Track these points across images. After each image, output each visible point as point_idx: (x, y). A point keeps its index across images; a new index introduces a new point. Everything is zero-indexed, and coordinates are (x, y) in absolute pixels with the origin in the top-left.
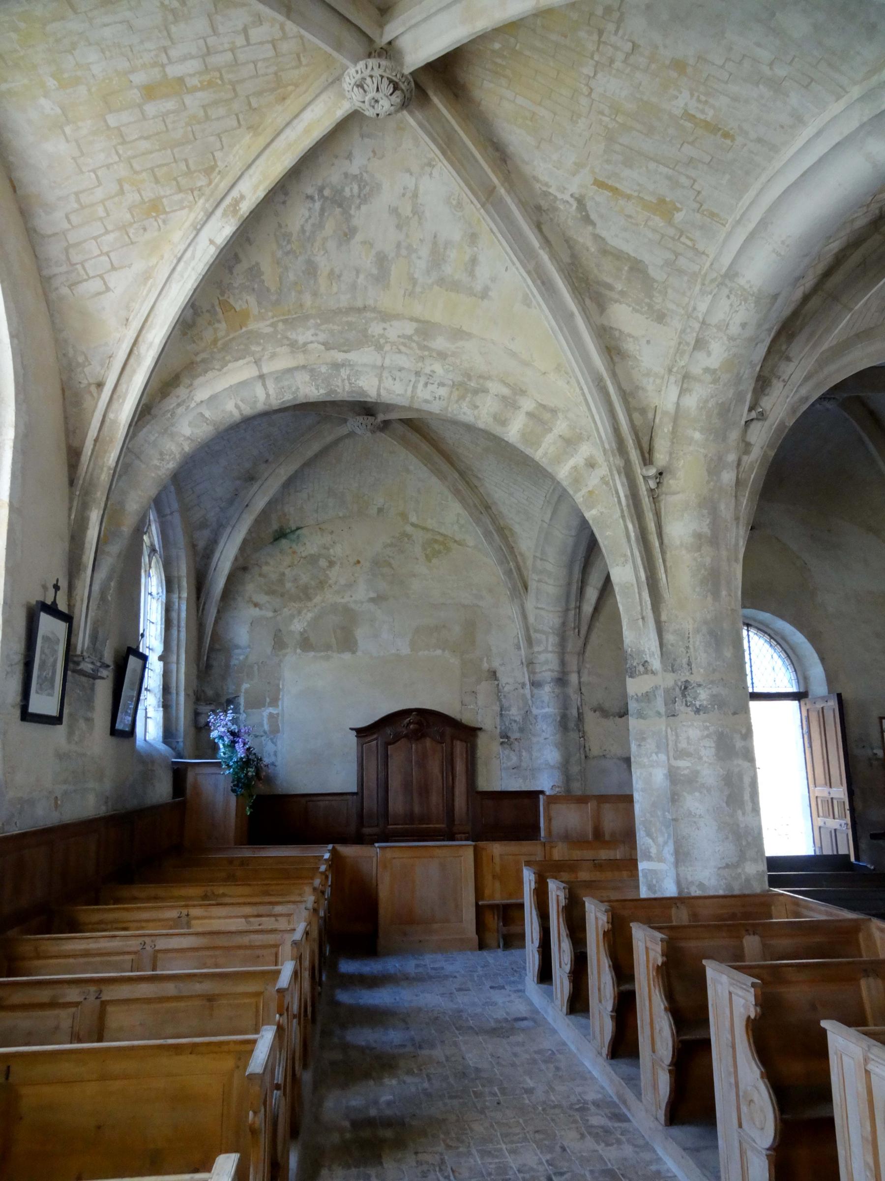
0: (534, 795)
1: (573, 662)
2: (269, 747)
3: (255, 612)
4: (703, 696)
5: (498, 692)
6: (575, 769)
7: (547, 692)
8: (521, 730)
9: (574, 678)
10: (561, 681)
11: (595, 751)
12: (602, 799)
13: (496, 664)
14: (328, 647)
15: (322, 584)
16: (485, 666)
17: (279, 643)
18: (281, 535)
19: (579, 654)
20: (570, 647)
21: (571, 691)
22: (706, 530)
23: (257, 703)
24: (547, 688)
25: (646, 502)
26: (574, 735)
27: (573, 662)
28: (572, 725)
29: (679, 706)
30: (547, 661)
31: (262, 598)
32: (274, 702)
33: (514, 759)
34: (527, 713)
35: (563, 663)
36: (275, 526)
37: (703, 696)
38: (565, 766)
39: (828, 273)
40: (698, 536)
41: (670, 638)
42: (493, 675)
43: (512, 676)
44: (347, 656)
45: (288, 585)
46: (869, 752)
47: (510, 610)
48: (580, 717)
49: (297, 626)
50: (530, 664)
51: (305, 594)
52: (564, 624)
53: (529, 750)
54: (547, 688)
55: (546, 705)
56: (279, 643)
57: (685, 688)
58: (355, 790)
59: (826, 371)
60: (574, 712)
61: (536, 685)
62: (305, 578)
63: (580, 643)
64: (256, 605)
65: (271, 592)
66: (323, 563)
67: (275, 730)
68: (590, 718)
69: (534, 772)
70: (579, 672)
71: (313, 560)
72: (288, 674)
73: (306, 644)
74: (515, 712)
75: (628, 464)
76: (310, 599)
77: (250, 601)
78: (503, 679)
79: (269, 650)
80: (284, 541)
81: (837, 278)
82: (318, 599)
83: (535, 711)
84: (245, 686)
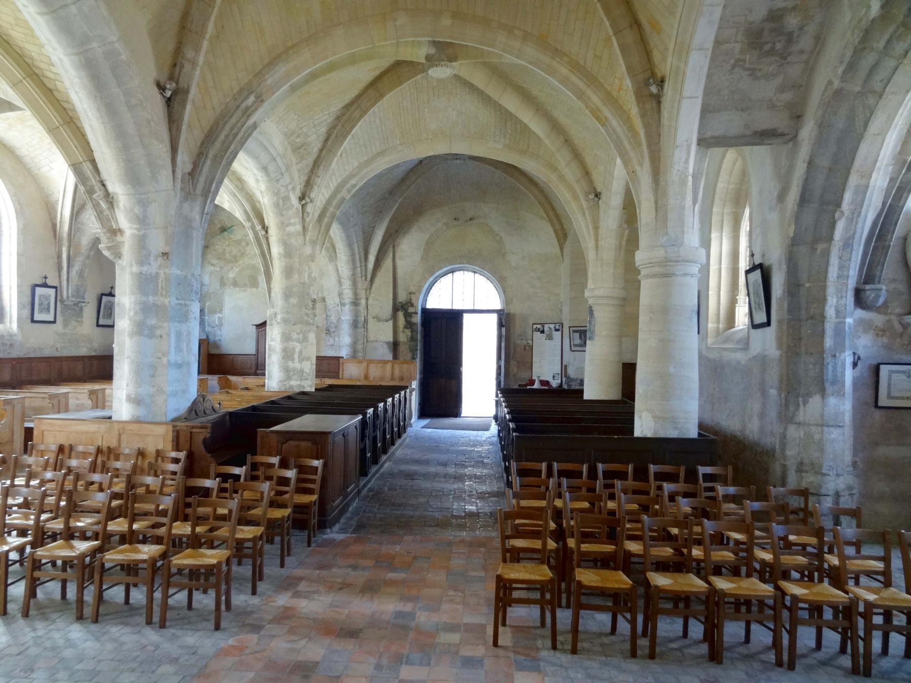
0: (338, 359)
1: (362, 294)
2: (219, 332)
3: (211, 268)
4: (279, 317)
5: (326, 309)
6: (360, 347)
7: (347, 308)
8: (336, 327)
9: (363, 302)
10: (355, 303)
11: (372, 338)
12: (370, 362)
13: (325, 294)
14: (245, 285)
15: (243, 254)
16: (320, 295)
17: (223, 283)
18: (223, 230)
19: (366, 290)
20: (360, 285)
21: (362, 308)
22: (282, 251)
23: (213, 312)
24: (347, 307)
25: (263, 241)
26: (361, 330)
27: (362, 294)
28: (360, 325)
29: (274, 322)
30: (348, 294)
31: (214, 261)
32: (221, 311)
33: (332, 341)
34: (340, 318)
35: (355, 294)
36: (219, 226)
37: (279, 317)
38: (354, 346)
39: (327, 140)
40: (279, 254)
41: (273, 294)
42: (324, 299)
43: (332, 300)
44: (254, 290)
45: (227, 255)
46: (525, 342)
47: (331, 267)
48: (366, 321)
49: (231, 275)
50: (340, 295)
51: (235, 259)
52: (354, 275)
53: (339, 337)
54: (347, 307)
55: (347, 316)
56: (223, 283)
57: (275, 314)
58: (254, 352)
59: (364, 172)
60: (363, 319)
61: (343, 305)
62: (235, 252)
63: (367, 284)
64: (212, 265)
65: (219, 259)
66: (243, 244)
67: (221, 325)
68: (371, 321)
69: (340, 347)
70: (367, 299)
71: (239, 242)
72: (227, 298)
73: (235, 284)
74: (333, 319)
75: (253, 224)
76: (237, 262)
77: (209, 262)
78: (329, 302)
79: (218, 287)
80: (225, 233)
81: (329, 143)
82: (241, 262)
83: (343, 318)
84: (208, 304)
